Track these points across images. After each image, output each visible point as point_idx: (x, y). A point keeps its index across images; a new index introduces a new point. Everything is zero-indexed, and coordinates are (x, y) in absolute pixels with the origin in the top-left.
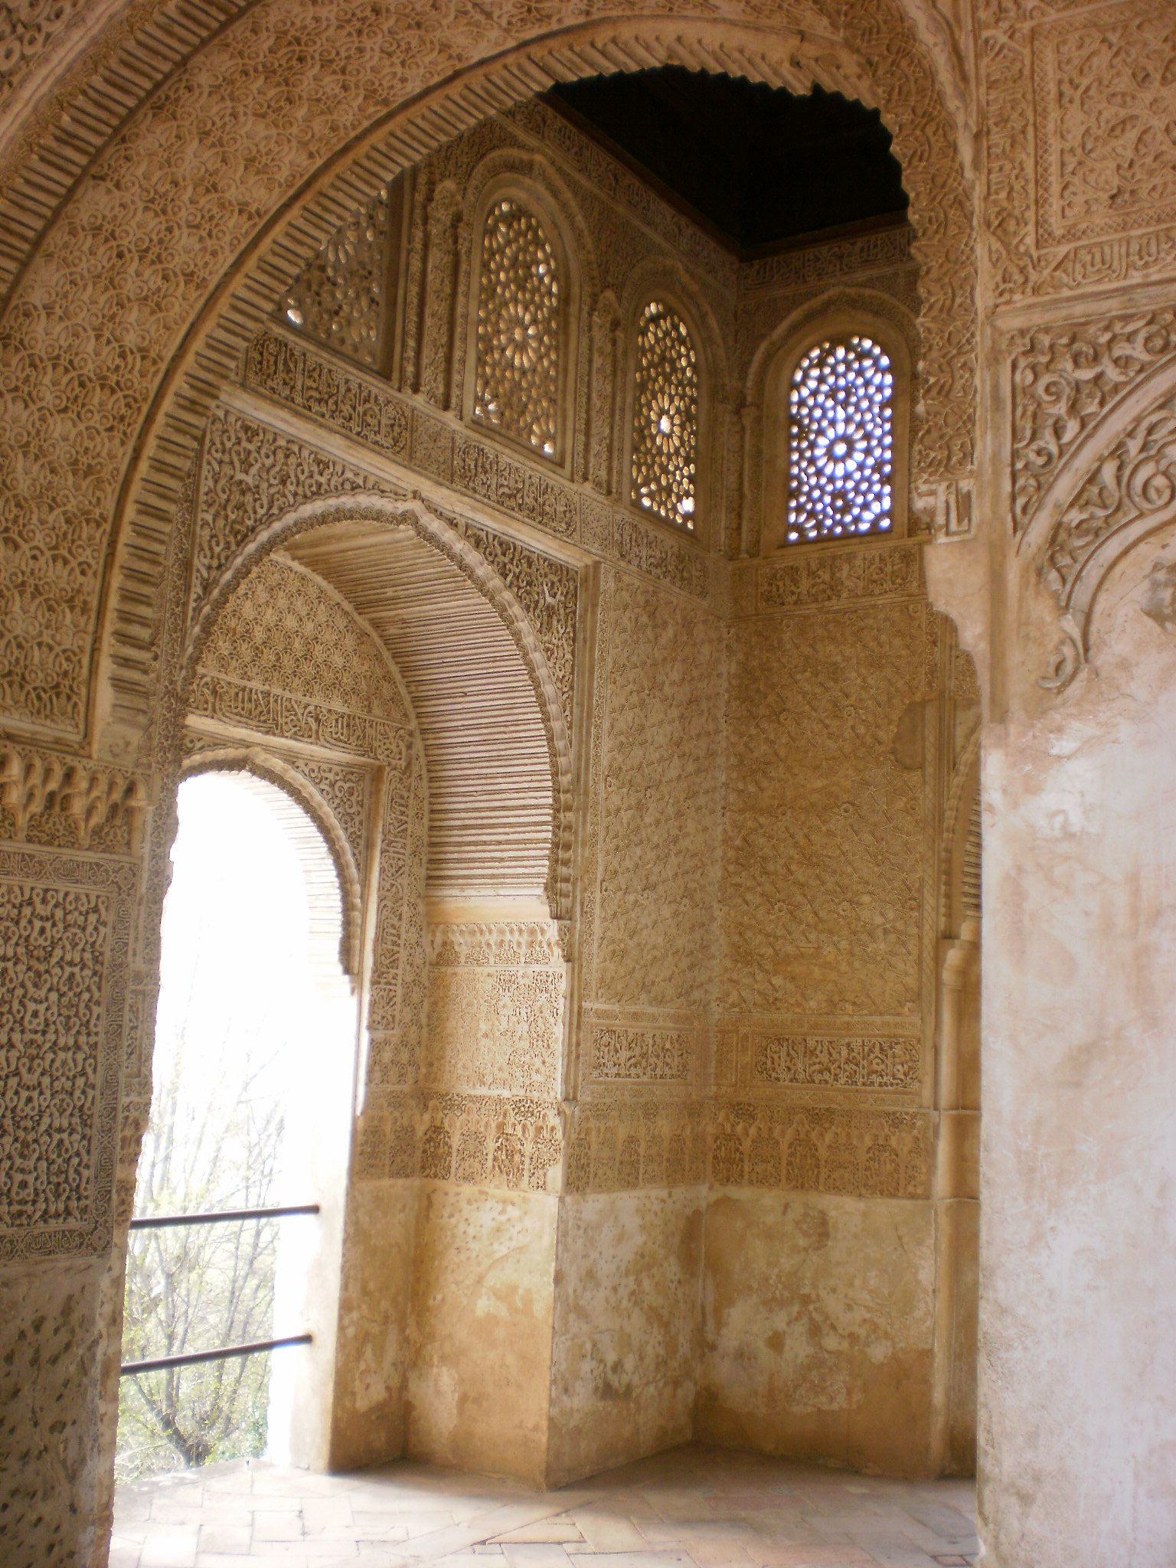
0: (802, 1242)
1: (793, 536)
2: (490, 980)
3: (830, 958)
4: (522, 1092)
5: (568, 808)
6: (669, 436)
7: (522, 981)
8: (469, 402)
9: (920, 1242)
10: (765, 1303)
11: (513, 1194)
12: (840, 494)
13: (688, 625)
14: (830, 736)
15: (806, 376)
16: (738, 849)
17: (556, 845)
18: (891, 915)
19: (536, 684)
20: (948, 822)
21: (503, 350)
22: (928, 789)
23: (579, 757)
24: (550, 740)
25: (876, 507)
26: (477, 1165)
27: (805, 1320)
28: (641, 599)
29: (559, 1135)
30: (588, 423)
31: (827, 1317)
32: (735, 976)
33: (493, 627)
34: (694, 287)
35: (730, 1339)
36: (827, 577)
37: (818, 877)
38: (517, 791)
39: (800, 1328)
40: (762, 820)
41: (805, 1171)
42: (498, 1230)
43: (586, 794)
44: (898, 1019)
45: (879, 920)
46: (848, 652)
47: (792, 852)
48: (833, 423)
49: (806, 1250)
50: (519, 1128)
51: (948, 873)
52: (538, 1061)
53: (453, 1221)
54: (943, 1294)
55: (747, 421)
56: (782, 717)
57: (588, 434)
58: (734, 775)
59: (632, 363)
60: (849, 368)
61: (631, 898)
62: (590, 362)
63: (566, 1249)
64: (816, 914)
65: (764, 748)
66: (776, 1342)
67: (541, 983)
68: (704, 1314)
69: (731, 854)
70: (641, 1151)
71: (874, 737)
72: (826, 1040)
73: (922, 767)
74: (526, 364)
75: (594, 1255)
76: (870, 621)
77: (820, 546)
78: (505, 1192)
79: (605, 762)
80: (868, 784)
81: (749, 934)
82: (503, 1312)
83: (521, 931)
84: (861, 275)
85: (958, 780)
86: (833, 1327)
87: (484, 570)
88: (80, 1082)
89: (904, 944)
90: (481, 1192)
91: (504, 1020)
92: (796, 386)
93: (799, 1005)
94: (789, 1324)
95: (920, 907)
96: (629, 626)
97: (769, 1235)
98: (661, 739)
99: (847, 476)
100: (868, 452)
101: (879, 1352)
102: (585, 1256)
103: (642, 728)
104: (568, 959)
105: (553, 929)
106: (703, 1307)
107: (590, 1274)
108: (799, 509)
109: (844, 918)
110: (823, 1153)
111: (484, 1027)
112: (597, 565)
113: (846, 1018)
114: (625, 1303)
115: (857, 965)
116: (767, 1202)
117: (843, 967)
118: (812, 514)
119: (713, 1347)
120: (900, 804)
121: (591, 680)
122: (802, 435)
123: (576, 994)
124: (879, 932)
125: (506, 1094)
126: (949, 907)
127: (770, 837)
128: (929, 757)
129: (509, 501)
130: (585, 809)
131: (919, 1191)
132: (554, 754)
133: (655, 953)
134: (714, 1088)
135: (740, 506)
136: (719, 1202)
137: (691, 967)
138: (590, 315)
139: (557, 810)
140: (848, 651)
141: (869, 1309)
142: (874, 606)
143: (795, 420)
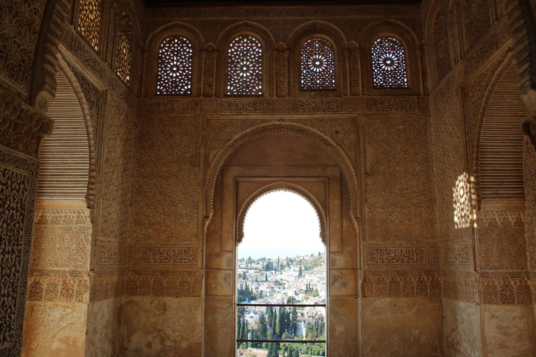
0: (158, 313)
1: (158, 93)
2: (61, 229)
3: (168, 223)
4: (74, 268)
5: (94, 171)
6: (125, 55)
7: (74, 230)
8: (77, 25)
9: (197, 310)
10: (145, 333)
11: (69, 304)
12: (176, 81)
13: (127, 116)
15: (164, 46)
16: (137, 189)
17: (89, 183)
18: (188, 211)
19: (87, 127)
20: (207, 183)
21: (86, 11)
23: (98, 154)
24: (90, 147)
25: (186, 88)
26: (54, 295)
27: (159, 337)
28: (117, 104)
29: (88, 283)
30: (107, 43)
31: (166, 335)
32: (135, 229)
33: (75, 105)
34: (134, 11)
35: (133, 346)
36: (170, 107)
37: (164, 198)
38: (75, 163)
39: (158, 340)
40: (145, 180)
41: (159, 290)
42: (62, 318)
43: (100, 166)
44: (191, 242)
45: (185, 212)
46: (176, 129)
47: (156, 190)
48: (173, 61)
49: (159, 315)
50: (72, 281)
51: (206, 198)
52: (80, 258)
53: (43, 315)
54: (203, 325)
55: (145, 57)
56: (153, 148)
57: (107, 47)
58: (136, 165)
59: (119, 29)
60: (178, 46)
61: (110, 202)
62: (109, 24)
63: (89, 322)
64: (164, 210)
66: (149, 345)
67: (82, 231)
68: (123, 338)
69: (134, 190)
70: (109, 286)
71: (184, 156)
72: (166, 249)
73: (199, 166)
74: (92, 19)
75: (96, 323)
78: (65, 304)
79: (105, 156)
80: (181, 170)
81: (140, 216)
82: (64, 346)
83: (74, 212)
84: (185, 19)
85: (210, 171)
86: (169, 338)
87: (76, 84)
88: (13, 269)
89: (193, 219)
90: (55, 305)
91: (66, 244)
92: (161, 48)
93: (157, 238)
94: (153, 338)
95: (198, 208)
96: (114, 112)
97: (146, 311)
98: (119, 151)
99: (177, 77)
100: (184, 71)
101: (184, 345)
102: (94, 324)
103: (114, 147)
104: (92, 222)
105: (87, 212)
106: (123, 336)
107: (95, 330)
108: (161, 85)
110: (165, 284)
111: (58, 246)
112: (107, 91)
113: (173, 242)
114: (104, 338)
115: (177, 226)
116: (146, 301)
117: (172, 226)
119: (126, 349)
120: (192, 177)
121: (103, 128)
122: (163, 63)
123: (95, 235)
125: (67, 269)
126: (206, 208)
129: (86, 62)
130: (100, 171)
131: (197, 294)
132: (90, 152)
133: (115, 221)
134: (127, 265)
135: (141, 82)
136: (128, 302)
137: (123, 226)
138: (110, 9)
139: (90, 171)
140: (176, 129)
141: (180, 332)
143: (161, 58)
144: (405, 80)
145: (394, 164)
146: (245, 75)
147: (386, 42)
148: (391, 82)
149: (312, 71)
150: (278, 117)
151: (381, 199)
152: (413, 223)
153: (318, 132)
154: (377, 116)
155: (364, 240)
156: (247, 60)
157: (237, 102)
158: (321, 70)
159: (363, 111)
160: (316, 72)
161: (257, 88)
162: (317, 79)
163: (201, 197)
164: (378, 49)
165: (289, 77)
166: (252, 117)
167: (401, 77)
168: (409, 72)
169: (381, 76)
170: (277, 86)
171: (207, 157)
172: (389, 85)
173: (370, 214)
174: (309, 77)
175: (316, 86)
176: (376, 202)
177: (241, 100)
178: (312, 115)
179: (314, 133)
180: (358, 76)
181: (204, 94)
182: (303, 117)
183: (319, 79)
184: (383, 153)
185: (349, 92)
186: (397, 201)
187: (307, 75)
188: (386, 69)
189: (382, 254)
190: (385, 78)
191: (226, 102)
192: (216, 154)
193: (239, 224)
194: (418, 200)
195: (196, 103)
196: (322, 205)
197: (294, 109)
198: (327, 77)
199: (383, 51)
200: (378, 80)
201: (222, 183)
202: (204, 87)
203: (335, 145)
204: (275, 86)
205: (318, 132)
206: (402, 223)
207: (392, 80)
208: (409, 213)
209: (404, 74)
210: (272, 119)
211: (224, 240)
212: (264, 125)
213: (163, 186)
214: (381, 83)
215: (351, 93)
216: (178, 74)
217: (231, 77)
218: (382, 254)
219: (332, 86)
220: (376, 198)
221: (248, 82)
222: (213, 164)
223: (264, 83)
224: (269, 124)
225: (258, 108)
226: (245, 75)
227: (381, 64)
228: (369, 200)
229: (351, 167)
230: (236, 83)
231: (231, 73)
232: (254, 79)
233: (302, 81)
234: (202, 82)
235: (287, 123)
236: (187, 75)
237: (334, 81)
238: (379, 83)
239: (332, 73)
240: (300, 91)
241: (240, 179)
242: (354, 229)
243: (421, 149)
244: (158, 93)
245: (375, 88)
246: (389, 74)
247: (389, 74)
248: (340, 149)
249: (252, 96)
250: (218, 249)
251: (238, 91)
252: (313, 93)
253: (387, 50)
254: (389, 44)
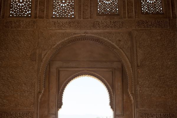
1: (11, 15)
3: (16, 96)
14: (17, 54)
18: (29, 88)
20: (40, 71)
22: (36, 65)
25: (28, 12)
36: (18, 24)
44: (30, 108)
45: (26, 89)
47: (9, 75)
65: (3, 55)
73: (36, 61)
76: (26, 33)
77: (17, 18)
89: (31, 94)
95: (34, 87)
99: (22, 6)
108: (12, 11)
109: (19, 89)
113: (19, 108)
115: (21, 98)
117: (19, 98)
118: (15, 12)
124: (26, 91)
126: (40, 87)
127: (4, 72)
128: (37, 59)
142: (27, 30)
144: (161, 9)
145: (155, 60)
146: (64, 5)
148: (153, 10)
149: (104, 3)
150: (83, 31)
151: (147, 82)
152: (167, 97)
153: (108, 40)
154: (144, 31)
155: (137, 107)
157: (59, 22)
158: (110, 3)
159: (135, 28)
160: (107, 4)
161: (71, 13)
162: (108, 8)
163: (37, 80)
165: (91, 6)
166: (68, 31)
167: (158, 7)
168: (163, 4)
169: (146, 6)
170: (83, 12)
171: (40, 55)
172: (151, 12)
173: (141, 91)
174: (102, 7)
175: (107, 12)
176: (144, 84)
177: (61, 20)
178: (105, 30)
179: (105, 41)
180: (132, 6)
181: (39, 16)
182: (99, 31)
183: (108, 8)
184: (148, 53)
185: (127, 16)
186: (157, 84)
187: (101, 6)
189: (148, 116)
190: (148, 8)
191: (53, 21)
192: (46, 54)
193: (60, 97)
194: (170, 83)
195: (34, 22)
196: (110, 85)
197: (94, 26)
198: (113, 7)
200: (145, 9)
201: (49, 71)
202: (39, 12)
203: (119, 48)
204: (82, 12)
205: (108, 41)
206: (160, 97)
207: (153, 9)
208: (164, 91)
209: (160, 5)
210: (80, 32)
211: (50, 107)
212: (76, 36)
213: (13, 73)
214: (147, 10)
215: (128, 17)
216: (23, 4)
217: (55, 6)
218: (148, 116)
219: (116, 12)
220: (144, 81)
221: (66, 9)
222: (44, 59)
223: (76, 10)
224: (78, 35)
225: (71, 25)
226: (64, 5)
228: (140, 83)
229: (129, 62)
230: (59, 10)
231: (56, 4)
232: (69, 8)
233: (99, 9)
234: (38, 9)
235: (89, 35)
237: (117, 9)
238: (145, 10)
239: (116, 5)
240: (97, 15)
241: (61, 69)
242: (131, 101)
243: (172, 51)
244: (11, 15)
245: (143, 13)
246: (151, 5)
247: (151, 5)
248: (122, 51)
249: (68, 18)
250: (47, 113)
251: (59, 15)
252: (105, 17)
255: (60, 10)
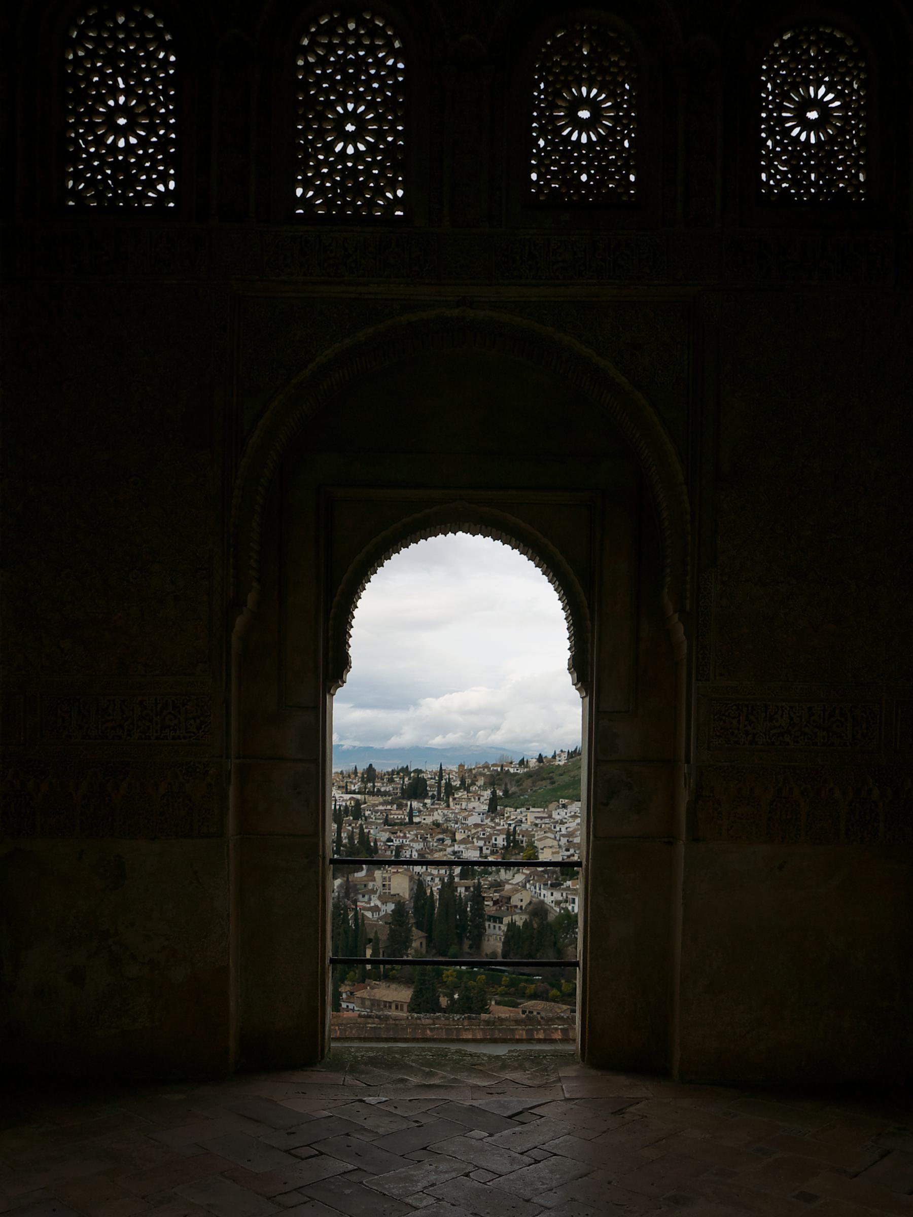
48: (114, 92)
143: (74, 80)
147: (811, 44)
156: (358, 99)
158: (594, 138)
164: (782, 67)
174: (555, 163)
175: (577, 192)
183: (585, 169)
188: (803, 137)
199: (799, 75)
217: (308, 157)
226: (350, 150)
227: (788, 119)
230: (324, 177)
232: (380, 165)
233: (534, 176)
236: (164, 142)
251: (328, 204)
253: (811, 72)
254: (820, 52)
255: (329, 176)
